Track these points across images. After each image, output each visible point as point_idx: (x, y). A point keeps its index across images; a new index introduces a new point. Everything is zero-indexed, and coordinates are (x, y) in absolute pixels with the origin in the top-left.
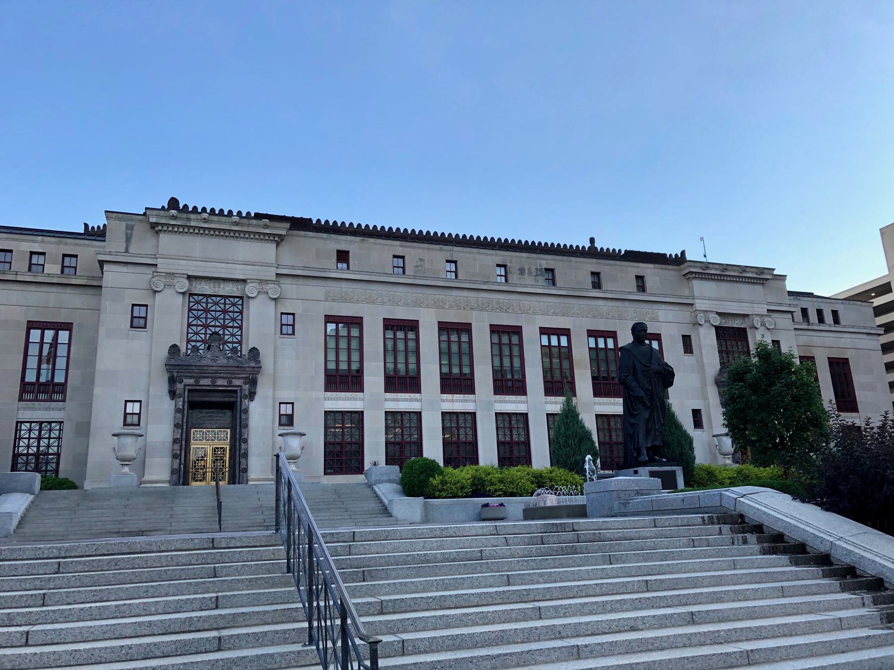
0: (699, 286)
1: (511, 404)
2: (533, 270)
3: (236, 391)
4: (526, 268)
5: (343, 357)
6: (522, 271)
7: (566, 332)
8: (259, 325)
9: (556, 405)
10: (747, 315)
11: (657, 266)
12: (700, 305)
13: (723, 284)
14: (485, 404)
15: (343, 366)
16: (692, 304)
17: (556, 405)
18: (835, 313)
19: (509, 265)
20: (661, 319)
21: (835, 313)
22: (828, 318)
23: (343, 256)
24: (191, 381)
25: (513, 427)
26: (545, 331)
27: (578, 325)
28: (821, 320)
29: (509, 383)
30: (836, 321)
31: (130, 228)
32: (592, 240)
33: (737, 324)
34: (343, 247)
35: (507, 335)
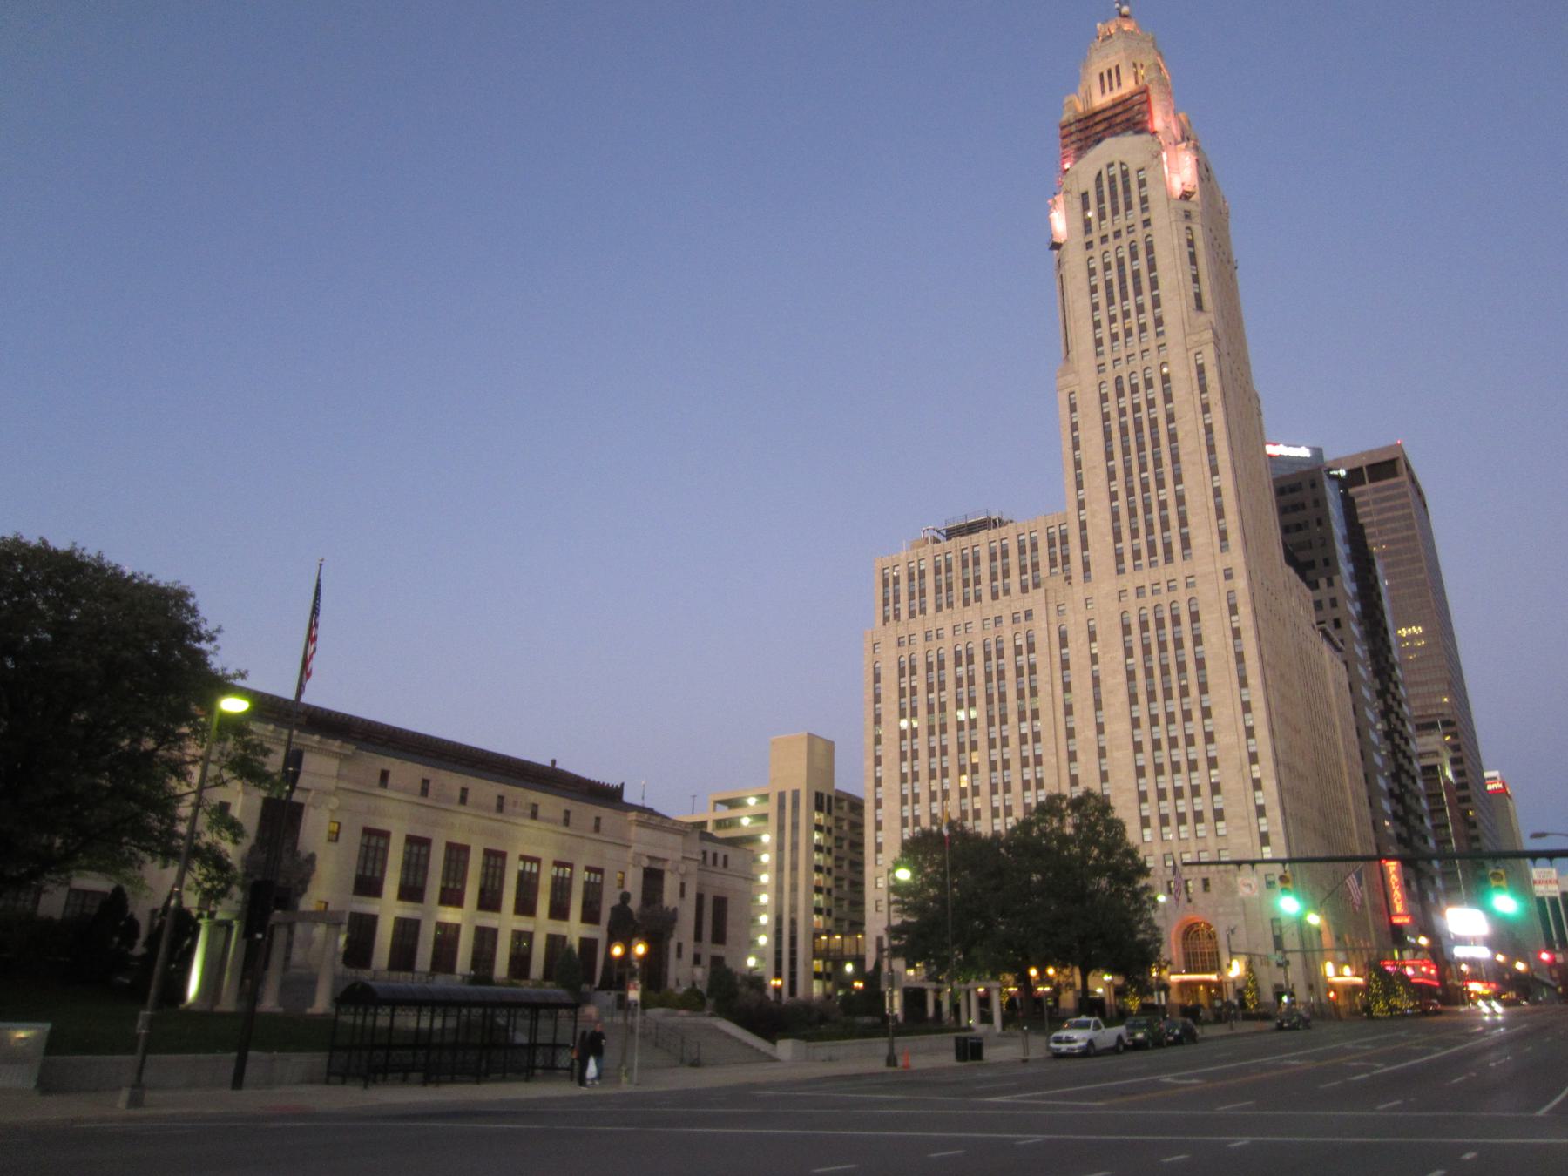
1: (488, 920)
5: (370, 865)
7: (537, 861)
8: (314, 832)
15: (368, 873)
18: (725, 857)
21: (725, 857)
22: (720, 861)
23: (384, 776)
25: (486, 938)
26: (524, 858)
27: (547, 854)
28: (715, 863)
29: (490, 901)
30: (725, 864)
32: (554, 762)
33: (658, 866)
34: (386, 767)
35: (495, 859)
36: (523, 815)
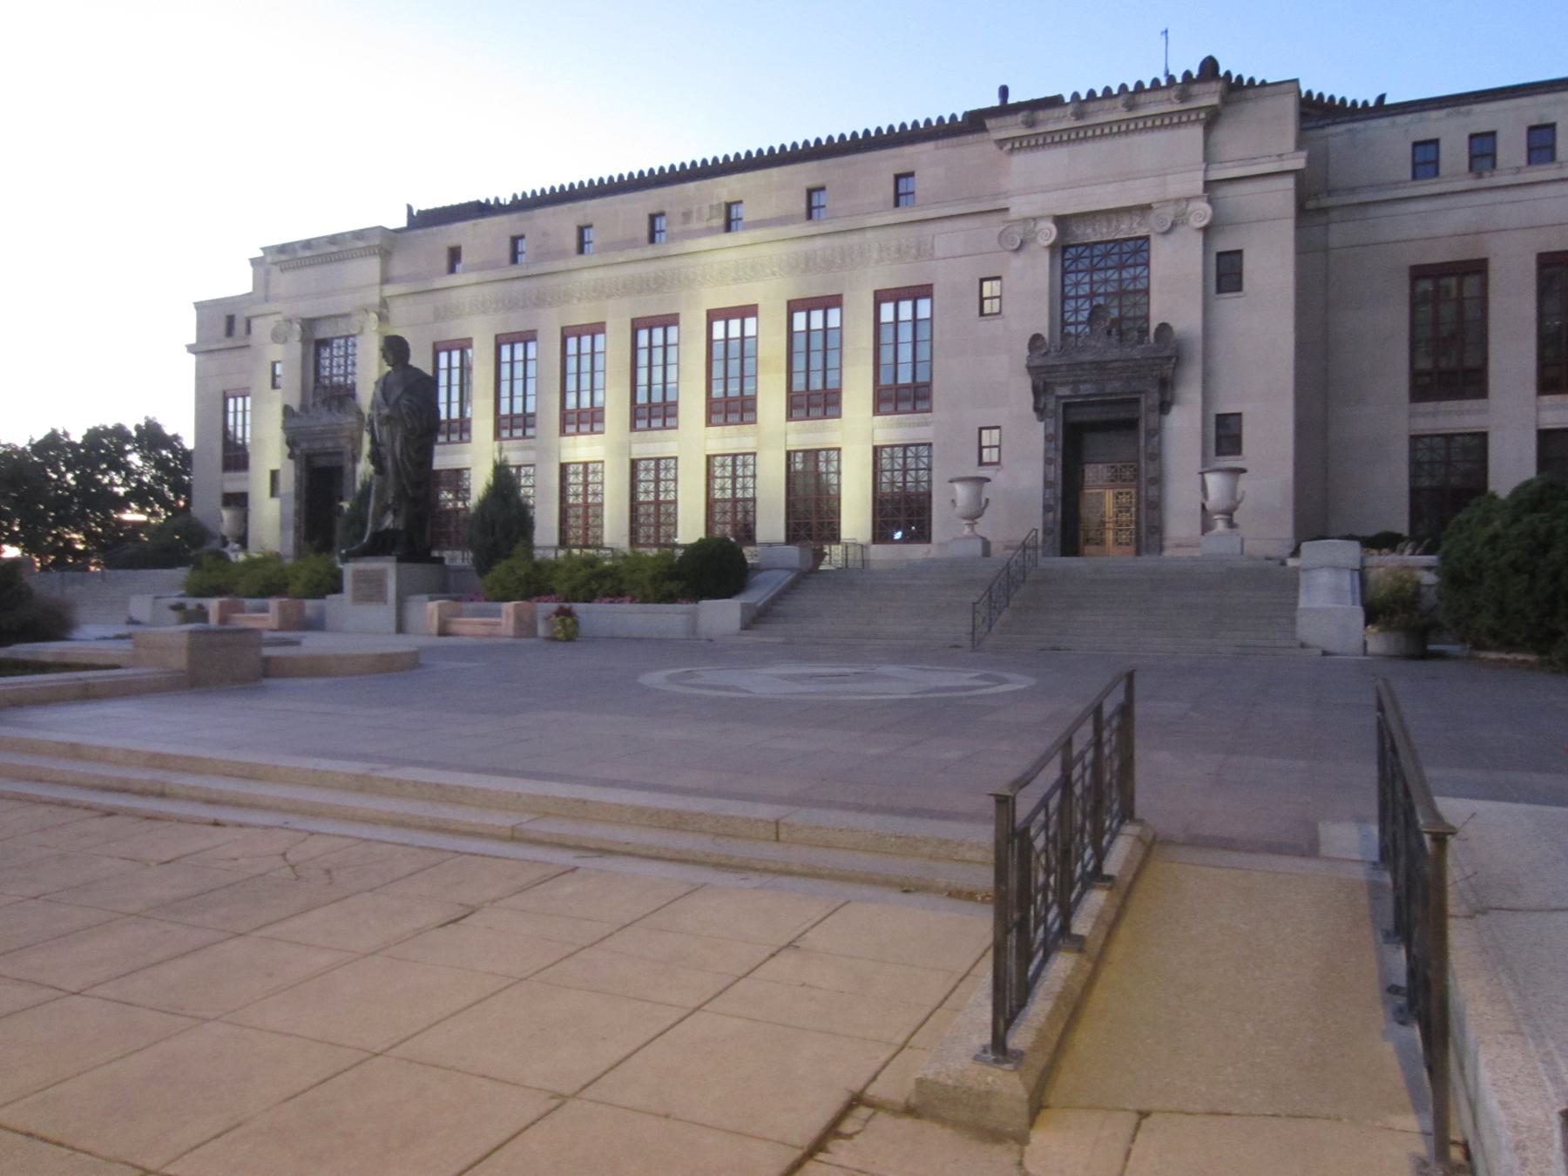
0: (1023, 165)
2: (706, 207)
3: (340, 454)
4: (695, 208)
6: (687, 216)
9: (889, 430)
10: (1148, 207)
11: (940, 143)
12: (1019, 208)
13: (1089, 149)
14: (693, 441)
16: (1007, 209)
17: (889, 430)
19: (667, 210)
20: (938, 253)
24: (304, 445)
31: (268, 273)
33: (1127, 228)
34: (453, 242)
36: (710, 231)
